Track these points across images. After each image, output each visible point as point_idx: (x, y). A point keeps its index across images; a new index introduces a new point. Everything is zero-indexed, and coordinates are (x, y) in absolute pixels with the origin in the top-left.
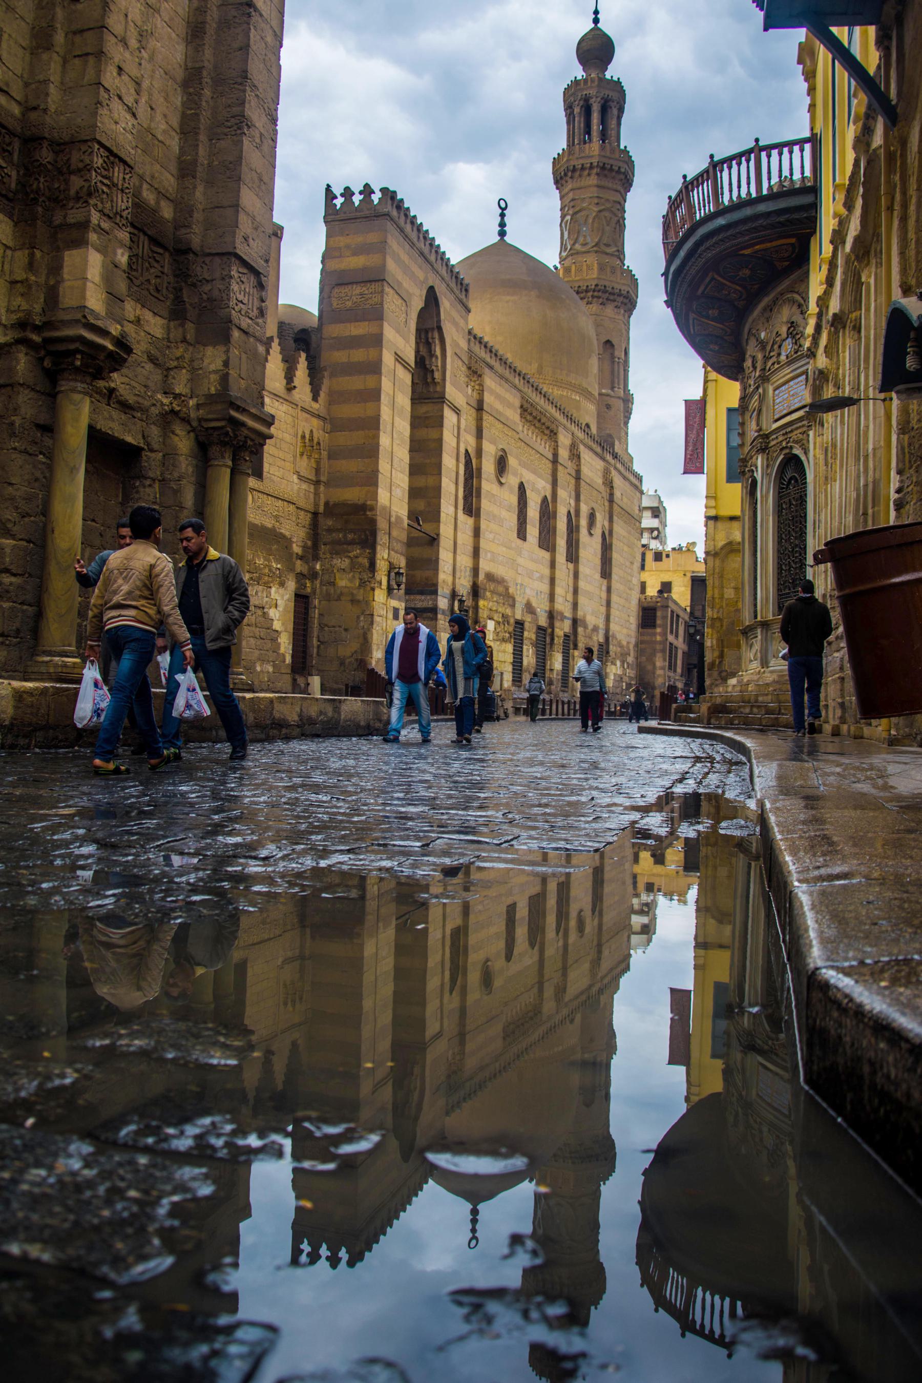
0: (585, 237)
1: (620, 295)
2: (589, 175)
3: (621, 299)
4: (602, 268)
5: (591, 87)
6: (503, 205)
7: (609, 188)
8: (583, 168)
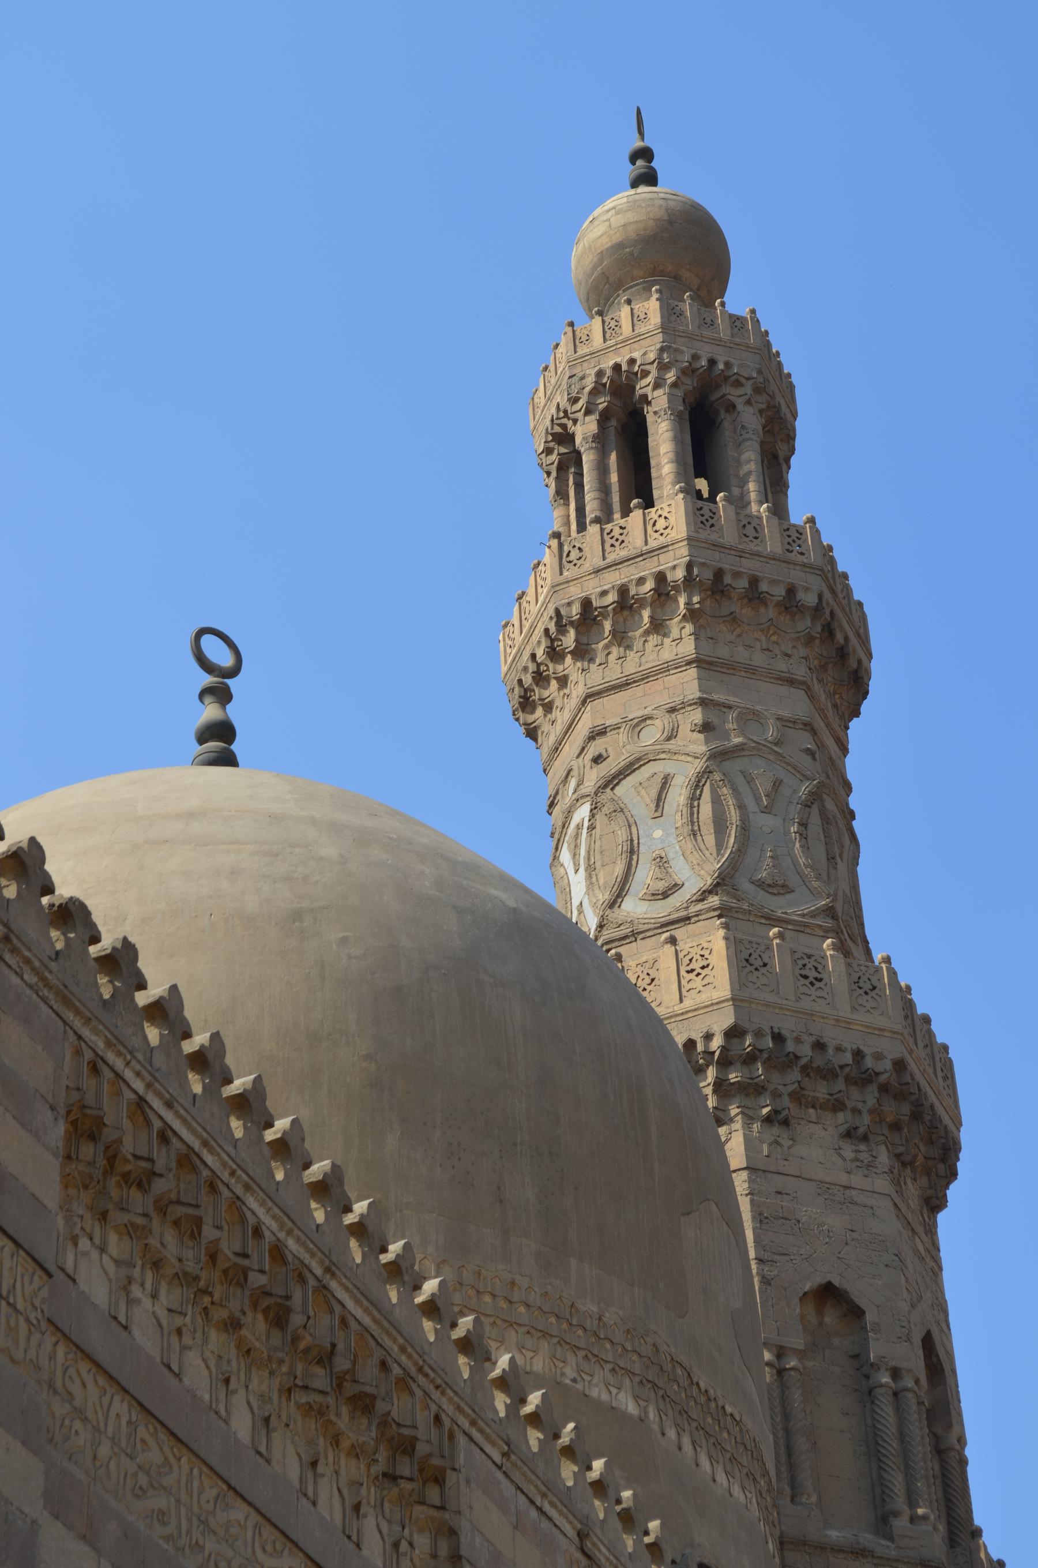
0: (661, 861)
1: (864, 1079)
2: (658, 627)
3: (871, 1096)
4: (746, 961)
5: (637, 338)
6: (218, 653)
7: (751, 671)
8: (626, 603)
